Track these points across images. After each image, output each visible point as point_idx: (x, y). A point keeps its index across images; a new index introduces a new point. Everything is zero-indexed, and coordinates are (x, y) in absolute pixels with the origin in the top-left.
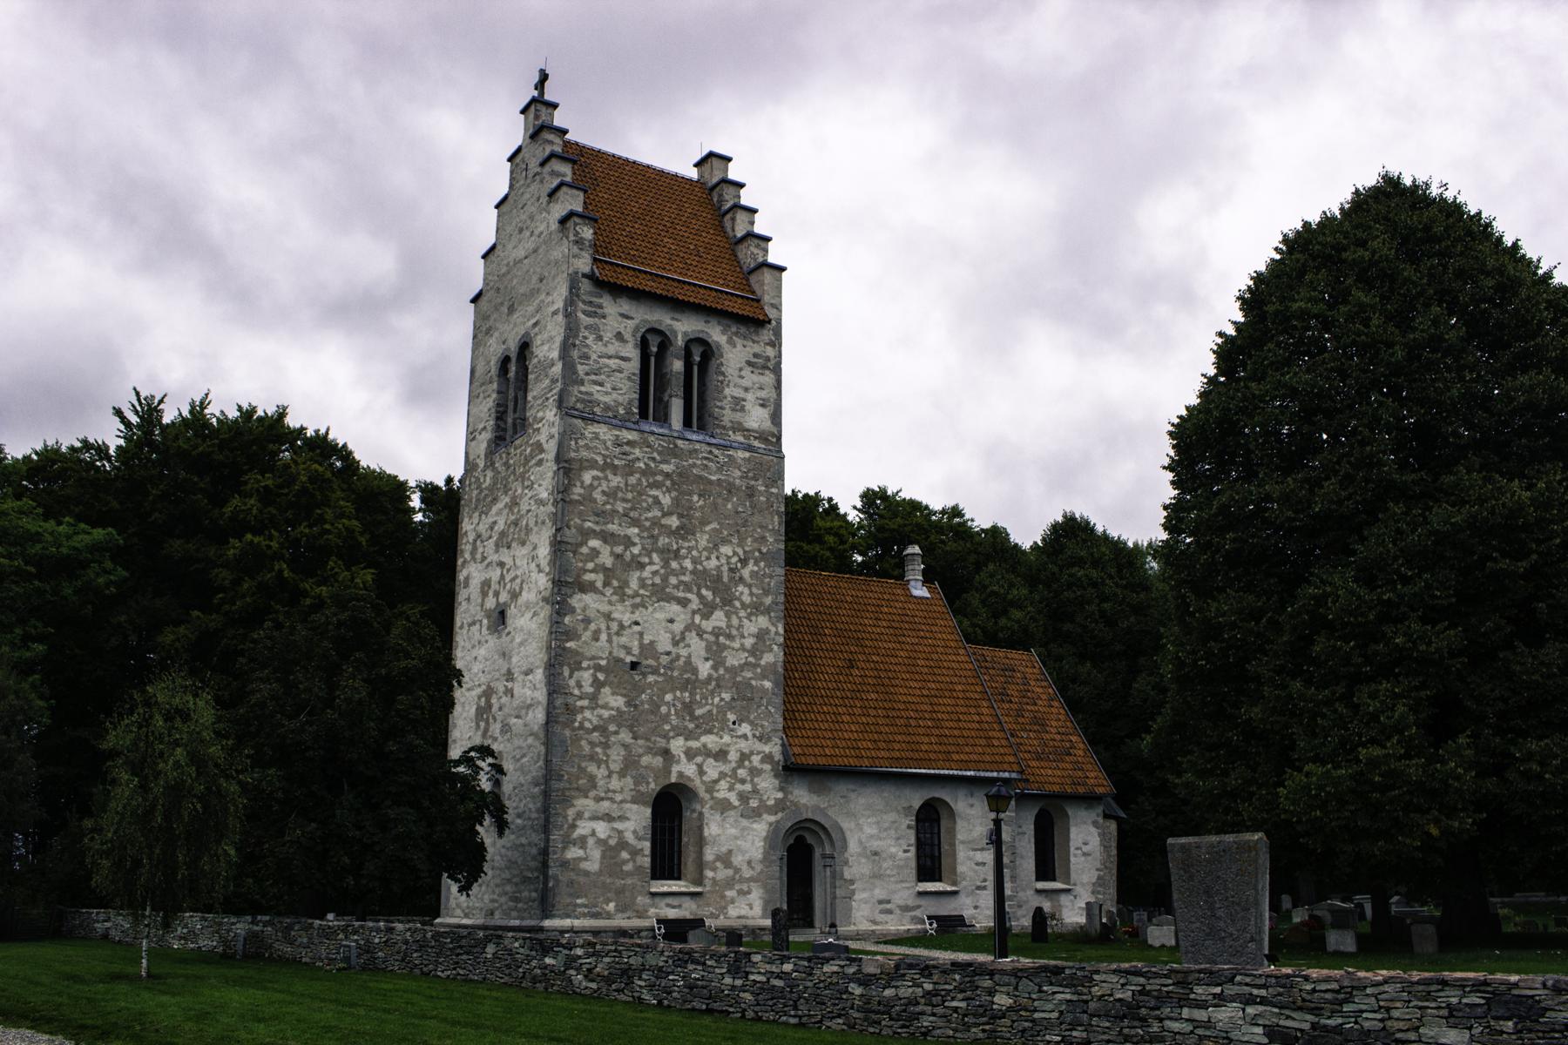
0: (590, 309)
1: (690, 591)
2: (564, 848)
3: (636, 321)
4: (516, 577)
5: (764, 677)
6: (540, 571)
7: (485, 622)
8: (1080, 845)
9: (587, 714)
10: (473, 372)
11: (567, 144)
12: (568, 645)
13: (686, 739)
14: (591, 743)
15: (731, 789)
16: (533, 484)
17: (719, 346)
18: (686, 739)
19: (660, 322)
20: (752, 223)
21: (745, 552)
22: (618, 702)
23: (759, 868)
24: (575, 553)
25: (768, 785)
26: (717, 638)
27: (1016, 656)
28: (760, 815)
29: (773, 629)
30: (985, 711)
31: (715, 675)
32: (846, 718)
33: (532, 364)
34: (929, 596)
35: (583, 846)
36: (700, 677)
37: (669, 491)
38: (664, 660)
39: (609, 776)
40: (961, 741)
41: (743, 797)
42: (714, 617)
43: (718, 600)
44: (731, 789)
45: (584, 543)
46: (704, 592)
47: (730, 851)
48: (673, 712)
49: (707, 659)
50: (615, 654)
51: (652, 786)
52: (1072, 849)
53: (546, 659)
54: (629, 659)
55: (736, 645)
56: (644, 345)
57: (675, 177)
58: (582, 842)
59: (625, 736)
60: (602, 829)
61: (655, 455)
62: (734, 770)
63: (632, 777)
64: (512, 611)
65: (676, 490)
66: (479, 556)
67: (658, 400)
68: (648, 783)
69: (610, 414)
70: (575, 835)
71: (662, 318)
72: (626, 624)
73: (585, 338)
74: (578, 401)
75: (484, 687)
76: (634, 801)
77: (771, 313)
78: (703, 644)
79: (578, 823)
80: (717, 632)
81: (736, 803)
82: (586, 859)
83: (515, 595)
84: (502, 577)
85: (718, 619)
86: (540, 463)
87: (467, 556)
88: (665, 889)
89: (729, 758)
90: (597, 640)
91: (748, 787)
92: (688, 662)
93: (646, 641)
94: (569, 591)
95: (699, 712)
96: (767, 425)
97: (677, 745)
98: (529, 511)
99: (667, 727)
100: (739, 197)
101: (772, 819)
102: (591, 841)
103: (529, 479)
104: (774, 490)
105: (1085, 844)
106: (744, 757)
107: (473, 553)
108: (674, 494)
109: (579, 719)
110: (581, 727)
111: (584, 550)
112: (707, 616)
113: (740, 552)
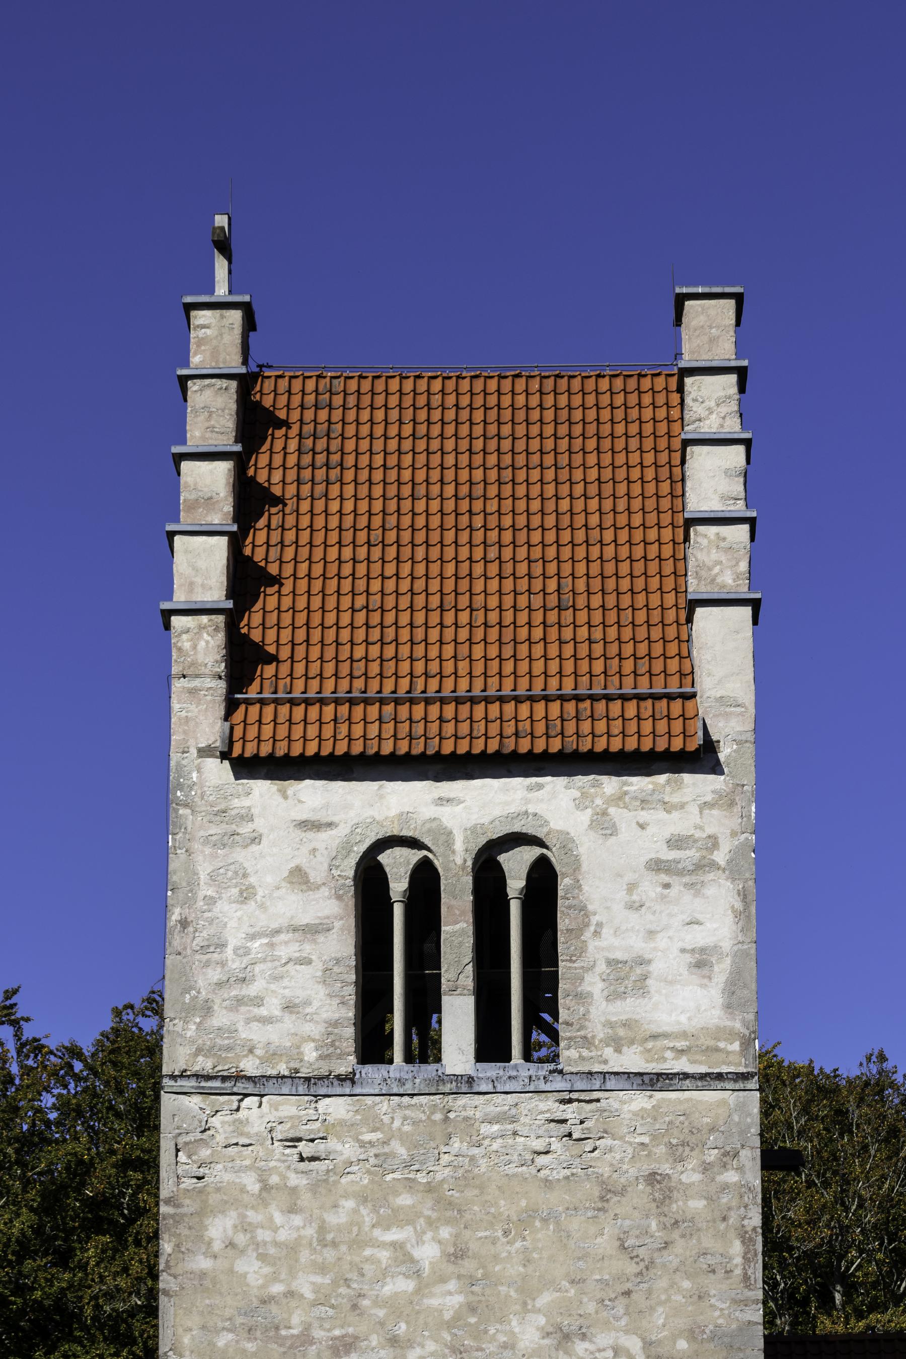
37: (431, 1223)
65: (448, 1222)
73: (211, 901)
74: (199, 1051)
108: (445, 1233)
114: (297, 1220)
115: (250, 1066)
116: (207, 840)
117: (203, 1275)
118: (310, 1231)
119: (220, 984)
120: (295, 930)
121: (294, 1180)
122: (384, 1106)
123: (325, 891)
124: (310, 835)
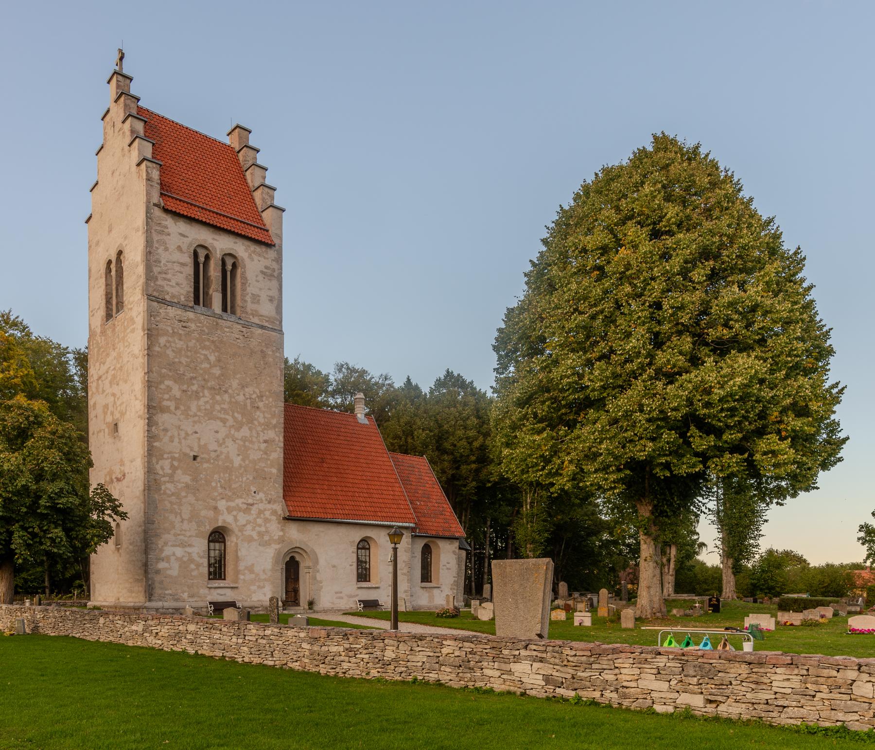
0: (159, 228)
1: (228, 414)
2: (157, 563)
3: (190, 239)
4: (123, 403)
5: (272, 466)
6: (136, 399)
7: (106, 430)
8: (445, 564)
9: (169, 485)
10: (90, 271)
11: (140, 109)
12: (155, 444)
13: (227, 501)
14: (171, 502)
15: (253, 529)
16: (129, 344)
17: (243, 260)
18: (227, 501)
19: (205, 240)
20: (264, 178)
21: (260, 392)
22: (187, 479)
23: (269, 573)
24: (156, 388)
25: (275, 528)
26: (244, 443)
27: (416, 459)
28: (270, 544)
29: (277, 438)
30: (397, 489)
31: (244, 464)
32: (319, 491)
33: (125, 265)
34: (368, 423)
35: (168, 561)
36: (234, 465)
37: (213, 351)
38: (213, 455)
39: (182, 522)
40: (383, 505)
41: (260, 534)
42: (242, 430)
43: (244, 420)
44: (253, 529)
45: (161, 382)
46: (236, 415)
47: (253, 565)
48: (219, 485)
49: (239, 455)
50: (184, 451)
51: (208, 527)
52: (441, 566)
53: (142, 452)
54: (192, 454)
55: (256, 447)
56: (196, 255)
57: (215, 141)
58: (167, 559)
59: (191, 498)
60: (179, 552)
61: (205, 328)
62: (255, 519)
63: (196, 522)
64: (120, 425)
65: (218, 351)
66: (100, 390)
67: (206, 293)
68: (205, 526)
69: (176, 301)
70: (163, 555)
71: (204, 236)
72: (190, 433)
73: (157, 248)
74: (154, 290)
75: (108, 470)
76: (197, 536)
77: (276, 241)
78: (236, 446)
79: (165, 548)
80: (244, 439)
81: (256, 537)
82: (170, 569)
83: (123, 414)
84: (115, 403)
85: (245, 432)
86: (133, 331)
87: (94, 390)
88: (216, 585)
89: (252, 512)
90: (173, 442)
91: (263, 529)
92: (227, 457)
93: (202, 443)
94: (154, 412)
95: (234, 486)
96: (273, 313)
97: (222, 504)
98: (128, 361)
99: (216, 494)
100: (256, 158)
101: (278, 546)
102: (173, 559)
103: (127, 341)
104: (278, 354)
105: (448, 563)
106: (261, 512)
107: (97, 388)
108: (217, 354)
109: (163, 488)
110: (165, 493)
111: (162, 386)
112: (238, 430)
113: (257, 391)
114: (182, 343)
115: (168, 298)
116: (156, 230)
117: (158, 352)
118: (184, 346)
119: (160, 273)
120: (179, 263)
121: (181, 332)
122: (202, 317)
123: (186, 255)
124: (182, 238)
